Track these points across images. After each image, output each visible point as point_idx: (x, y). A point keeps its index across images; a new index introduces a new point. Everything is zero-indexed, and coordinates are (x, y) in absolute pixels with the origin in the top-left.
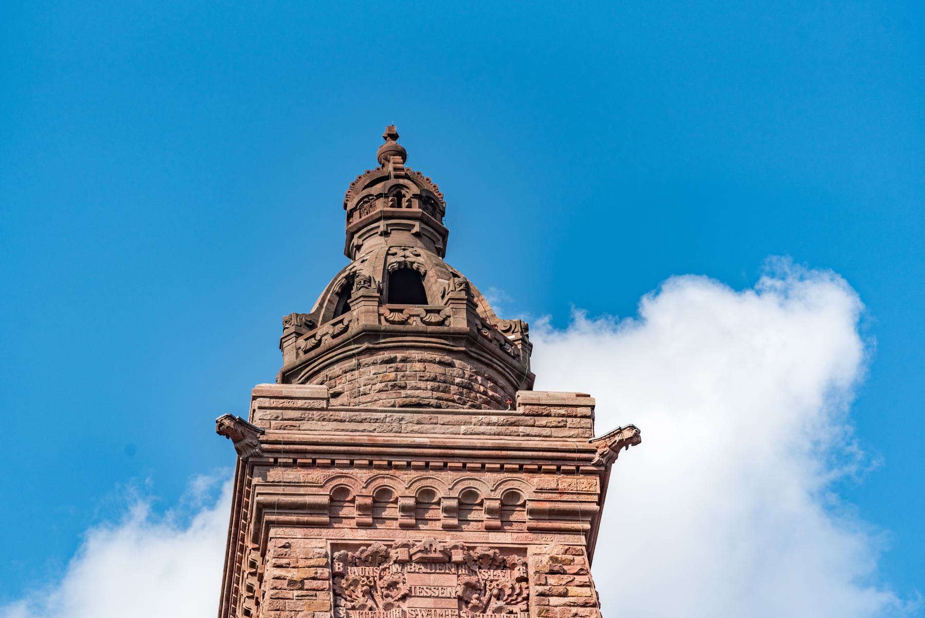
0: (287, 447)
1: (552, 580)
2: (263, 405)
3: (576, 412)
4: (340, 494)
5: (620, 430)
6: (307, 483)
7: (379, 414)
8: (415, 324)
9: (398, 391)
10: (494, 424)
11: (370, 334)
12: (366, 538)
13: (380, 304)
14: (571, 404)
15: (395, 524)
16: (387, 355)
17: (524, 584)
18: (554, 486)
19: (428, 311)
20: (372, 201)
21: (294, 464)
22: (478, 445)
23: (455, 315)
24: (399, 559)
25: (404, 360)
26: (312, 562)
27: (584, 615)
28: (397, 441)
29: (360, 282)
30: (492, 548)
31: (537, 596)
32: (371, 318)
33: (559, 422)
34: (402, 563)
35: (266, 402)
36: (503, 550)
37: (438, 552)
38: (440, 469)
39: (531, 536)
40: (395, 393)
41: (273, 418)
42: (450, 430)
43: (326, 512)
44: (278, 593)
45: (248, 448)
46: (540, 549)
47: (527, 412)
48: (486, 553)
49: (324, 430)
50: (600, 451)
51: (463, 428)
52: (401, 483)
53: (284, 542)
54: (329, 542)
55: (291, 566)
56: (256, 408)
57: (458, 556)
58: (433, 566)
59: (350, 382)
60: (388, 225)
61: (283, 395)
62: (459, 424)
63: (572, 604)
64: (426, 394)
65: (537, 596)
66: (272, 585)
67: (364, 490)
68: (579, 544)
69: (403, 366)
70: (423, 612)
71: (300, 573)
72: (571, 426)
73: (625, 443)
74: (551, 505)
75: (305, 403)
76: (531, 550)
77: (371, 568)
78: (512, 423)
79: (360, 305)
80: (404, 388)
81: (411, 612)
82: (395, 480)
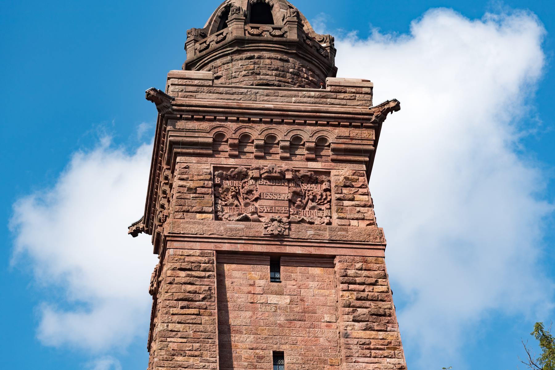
0: (188, 108)
1: (345, 191)
2: (174, 83)
3: (362, 91)
4: (219, 137)
5: (388, 102)
6: (200, 130)
7: (244, 90)
8: (266, 35)
9: (256, 76)
10: (312, 97)
11: (239, 42)
12: (234, 164)
13: (246, 23)
14: (359, 86)
15: (252, 156)
16: (249, 54)
17: (328, 193)
18: (347, 135)
19: (274, 29)
21: (192, 119)
22: (303, 109)
23: (290, 31)
24: (254, 176)
25: (259, 58)
26: (202, 177)
27: (364, 212)
28: (254, 106)
29: (234, 10)
31: (336, 200)
32: (240, 32)
33: (351, 97)
35: (176, 81)
37: (277, 173)
39: (333, 164)
40: (253, 77)
41: (180, 91)
42: (286, 100)
44: (180, 195)
45: (165, 108)
46: (338, 172)
47: (332, 90)
48: (306, 174)
49: (210, 99)
50: (375, 114)
51: (294, 99)
53: (185, 165)
54: (212, 165)
55: (189, 179)
56: (170, 85)
57: (289, 176)
58: (274, 181)
62: (291, 96)
63: (357, 205)
64: (271, 77)
65: (336, 200)
66: (178, 190)
67: (233, 135)
68: (362, 169)
69: (258, 61)
71: (194, 183)
73: (391, 110)
74: (345, 146)
75: (199, 82)
76: (333, 172)
77: (237, 181)
78: (323, 97)
79: (233, 24)
80: (259, 74)
81: (260, 208)
82: (252, 129)
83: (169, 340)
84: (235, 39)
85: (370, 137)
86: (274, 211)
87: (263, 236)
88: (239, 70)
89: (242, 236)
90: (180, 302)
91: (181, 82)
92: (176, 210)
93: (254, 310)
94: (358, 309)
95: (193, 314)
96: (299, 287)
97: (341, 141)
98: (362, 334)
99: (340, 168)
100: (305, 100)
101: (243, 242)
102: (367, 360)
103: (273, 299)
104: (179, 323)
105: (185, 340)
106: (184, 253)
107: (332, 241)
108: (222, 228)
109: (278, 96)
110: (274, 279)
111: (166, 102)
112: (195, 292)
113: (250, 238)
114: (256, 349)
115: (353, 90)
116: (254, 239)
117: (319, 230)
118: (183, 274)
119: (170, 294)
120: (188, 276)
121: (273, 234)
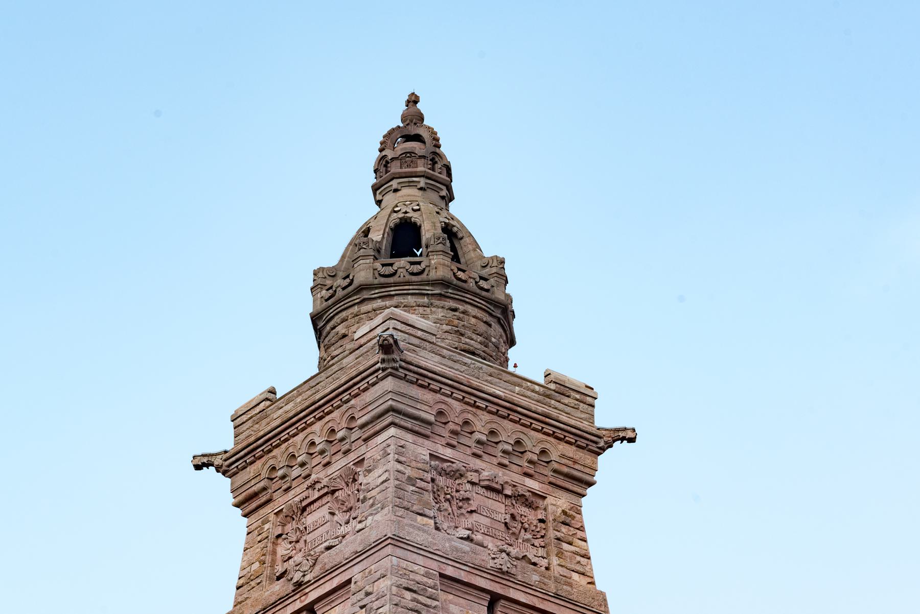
0: (416, 369)
1: (564, 529)
2: (397, 327)
5: (625, 429)
6: (423, 401)
7: (467, 359)
9: (460, 337)
12: (451, 457)
15: (469, 451)
16: (453, 304)
17: (543, 525)
18: (571, 455)
19: (459, 269)
20: (414, 158)
22: (533, 409)
24: (473, 481)
25: (464, 312)
26: (420, 465)
29: (439, 238)
30: (529, 491)
31: (555, 539)
32: (446, 271)
33: (575, 405)
34: (473, 484)
35: (400, 326)
36: (535, 494)
37: (499, 484)
39: (550, 488)
40: (457, 337)
41: (402, 339)
42: (510, 388)
43: (430, 428)
44: (400, 484)
46: (556, 501)
47: (557, 390)
48: (525, 494)
52: (479, 421)
53: (403, 443)
54: (429, 451)
56: (391, 327)
57: (508, 492)
58: (492, 493)
59: (422, 316)
60: (426, 183)
61: (409, 323)
62: (515, 384)
65: (555, 539)
66: (396, 476)
67: (456, 419)
69: (463, 317)
70: (484, 528)
71: (413, 472)
72: (582, 410)
73: (622, 439)
75: (423, 335)
76: (550, 500)
77: (451, 480)
78: (547, 395)
79: (439, 257)
80: (462, 335)
81: (477, 526)
82: (475, 417)
85: (593, 465)
86: (491, 534)
87: (490, 568)
88: (440, 322)
89: (468, 562)
91: (404, 328)
92: (396, 504)
97: (564, 461)
99: (557, 496)
100: (529, 393)
106: (408, 567)
107: (557, 596)
109: (501, 379)
111: (397, 355)
113: (476, 567)
115: (578, 396)
116: (479, 569)
117: (544, 577)
118: (408, 595)
120: (414, 600)
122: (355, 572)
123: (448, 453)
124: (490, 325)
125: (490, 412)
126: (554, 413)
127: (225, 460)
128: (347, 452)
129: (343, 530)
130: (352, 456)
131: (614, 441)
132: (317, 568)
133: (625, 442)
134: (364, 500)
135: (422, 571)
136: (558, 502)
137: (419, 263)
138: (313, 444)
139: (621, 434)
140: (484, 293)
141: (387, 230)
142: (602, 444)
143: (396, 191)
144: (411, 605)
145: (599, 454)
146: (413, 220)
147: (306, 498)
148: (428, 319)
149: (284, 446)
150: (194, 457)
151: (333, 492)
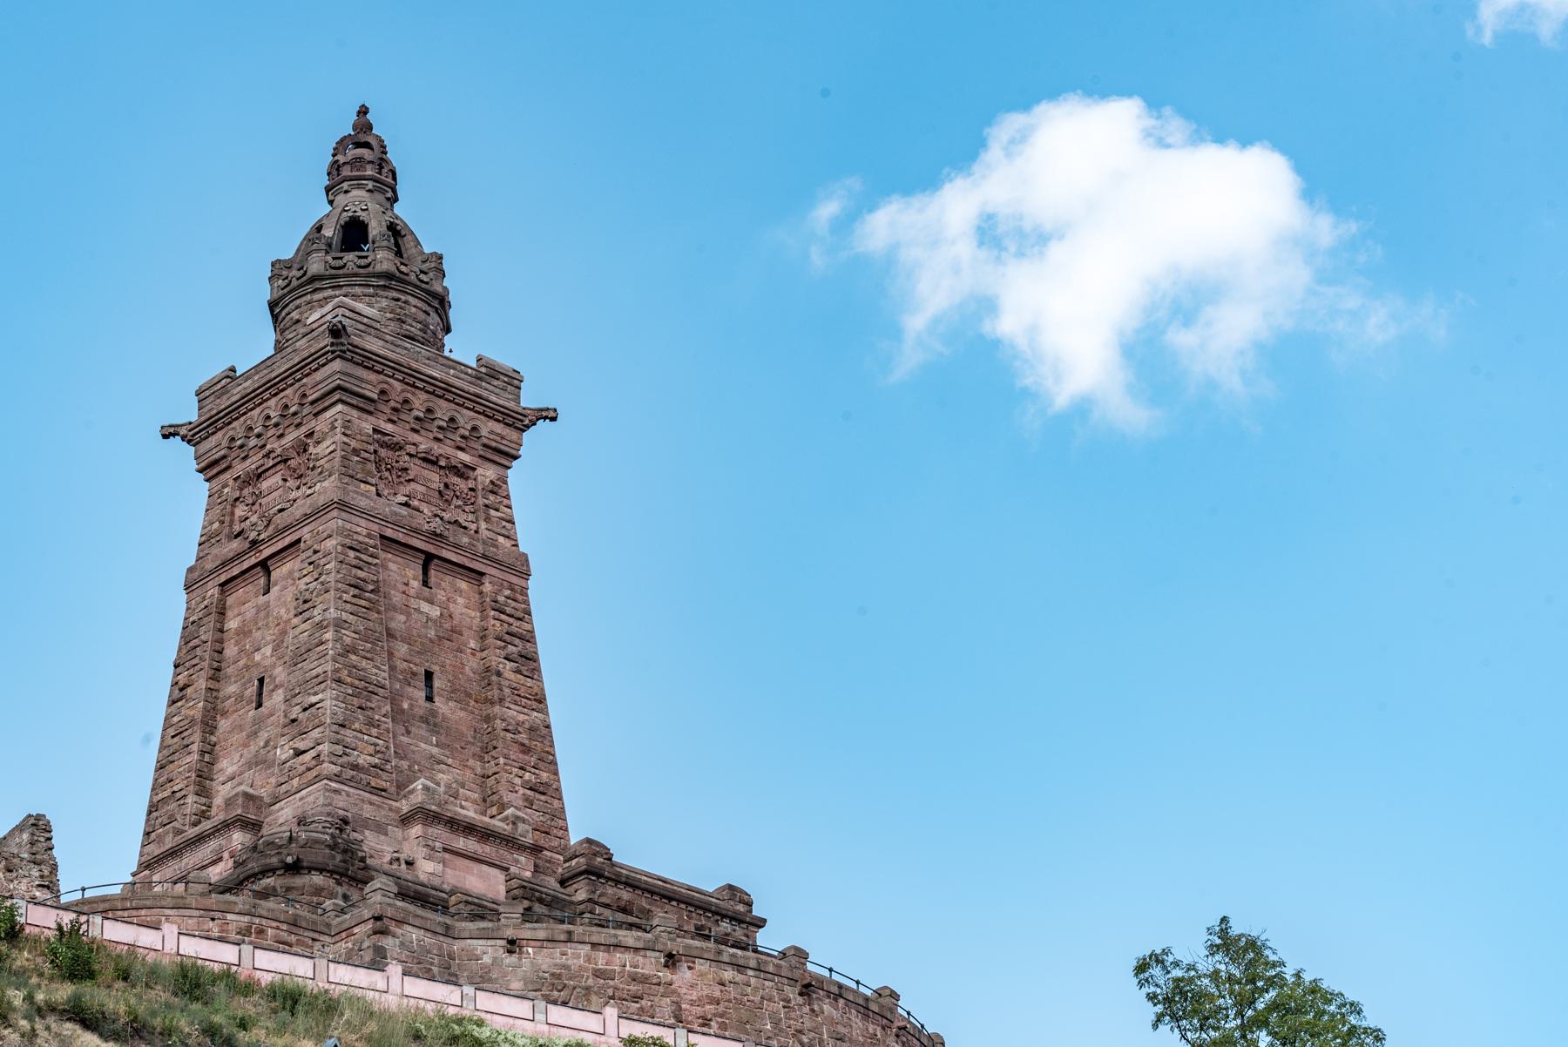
0: (362, 352)
1: (492, 497)
5: (548, 409)
10: (469, 375)
15: (408, 427)
16: (395, 294)
18: (500, 432)
19: (402, 264)
25: (406, 302)
34: (411, 455)
35: (348, 313)
36: (466, 466)
38: (439, 397)
53: (349, 418)
57: (443, 463)
60: (374, 186)
62: (450, 367)
64: (415, 330)
76: (479, 471)
80: (404, 322)
83: (343, 631)
84: (386, 273)
90: (352, 589)
93: (408, 615)
94: (509, 646)
95: (364, 607)
96: (448, 600)
97: (492, 437)
98: (512, 676)
101: (405, 531)
102: (517, 708)
103: (425, 607)
104: (351, 613)
105: (357, 636)
107: (484, 556)
108: (387, 509)
110: (425, 583)
112: (364, 581)
114: (410, 662)
115: (506, 379)
116: (416, 531)
118: (352, 554)
119: (342, 575)
121: (435, 532)
122: (305, 533)
123: (389, 427)
124: (429, 314)
125: (427, 392)
126: (485, 394)
127: (190, 431)
128: (298, 425)
129: (293, 495)
130: (303, 429)
131: (538, 420)
132: (271, 528)
133: (548, 420)
134: (314, 468)
135: (365, 532)
136: (487, 473)
137: (366, 257)
138: (268, 417)
139: (544, 414)
140: (424, 286)
141: (338, 227)
142: (527, 422)
143: (346, 192)
144: (354, 562)
145: (524, 431)
146: (361, 218)
147: (262, 465)
148: (373, 307)
149: (242, 419)
150: (162, 427)
151: (285, 461)
